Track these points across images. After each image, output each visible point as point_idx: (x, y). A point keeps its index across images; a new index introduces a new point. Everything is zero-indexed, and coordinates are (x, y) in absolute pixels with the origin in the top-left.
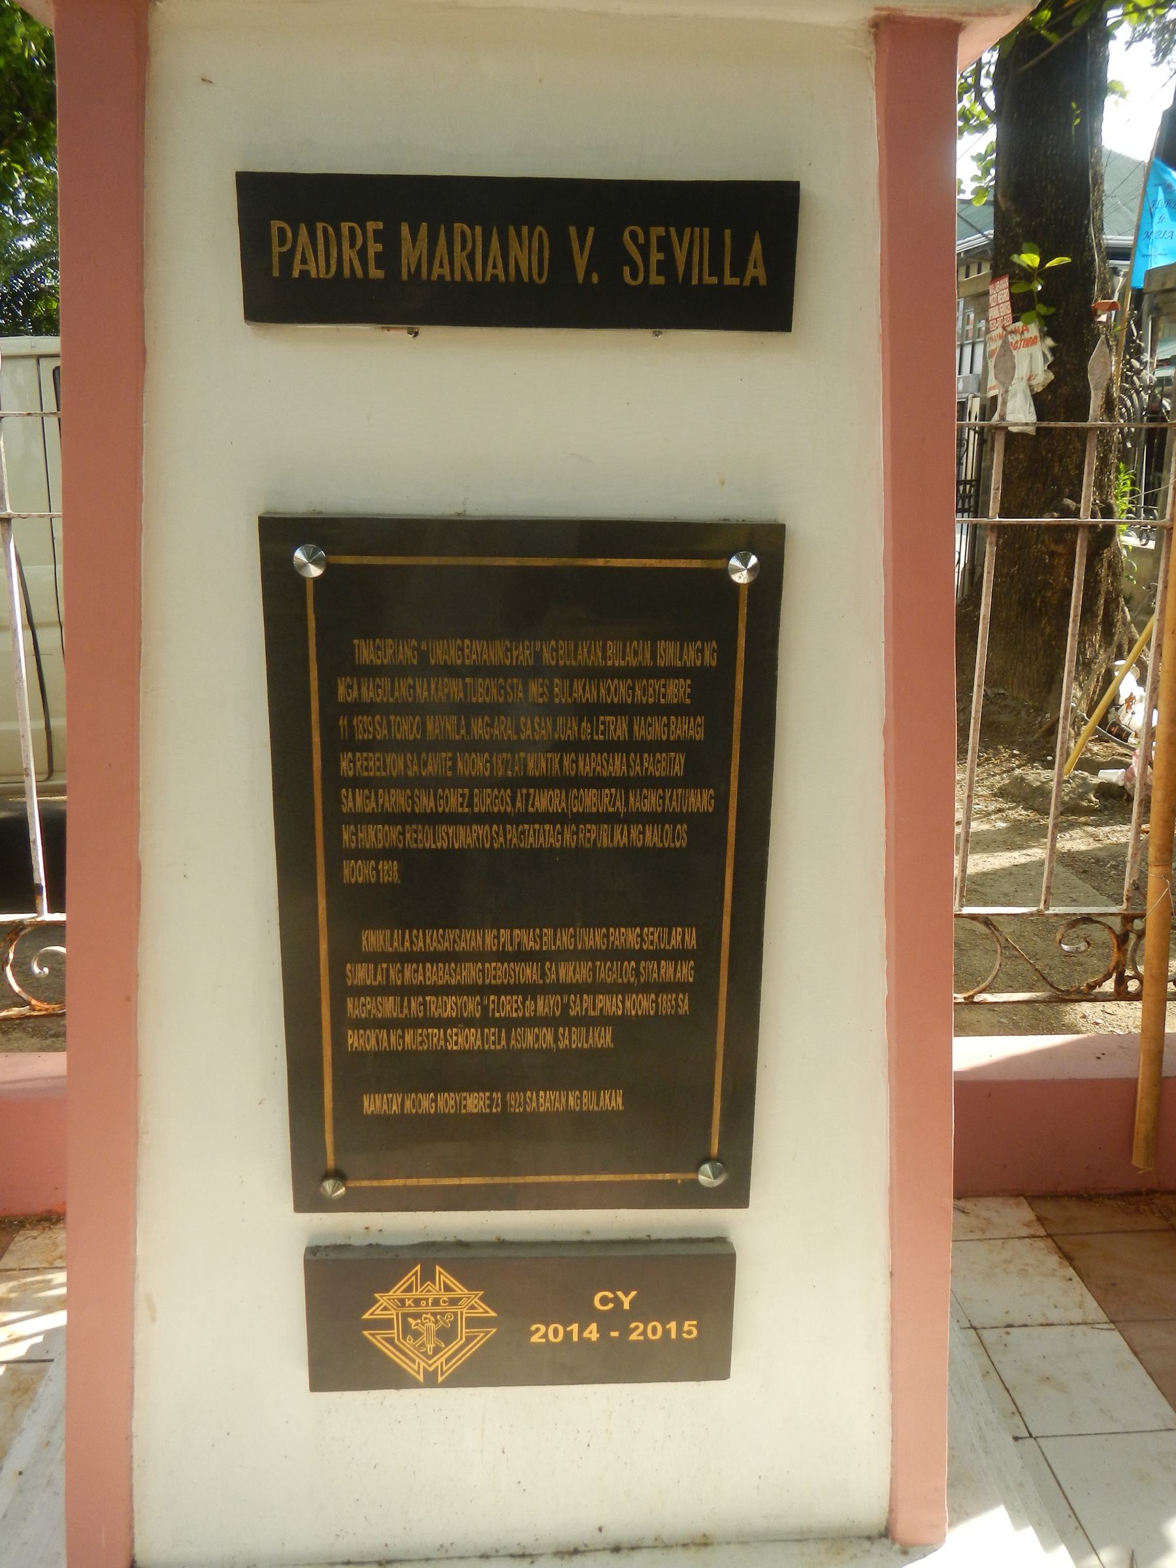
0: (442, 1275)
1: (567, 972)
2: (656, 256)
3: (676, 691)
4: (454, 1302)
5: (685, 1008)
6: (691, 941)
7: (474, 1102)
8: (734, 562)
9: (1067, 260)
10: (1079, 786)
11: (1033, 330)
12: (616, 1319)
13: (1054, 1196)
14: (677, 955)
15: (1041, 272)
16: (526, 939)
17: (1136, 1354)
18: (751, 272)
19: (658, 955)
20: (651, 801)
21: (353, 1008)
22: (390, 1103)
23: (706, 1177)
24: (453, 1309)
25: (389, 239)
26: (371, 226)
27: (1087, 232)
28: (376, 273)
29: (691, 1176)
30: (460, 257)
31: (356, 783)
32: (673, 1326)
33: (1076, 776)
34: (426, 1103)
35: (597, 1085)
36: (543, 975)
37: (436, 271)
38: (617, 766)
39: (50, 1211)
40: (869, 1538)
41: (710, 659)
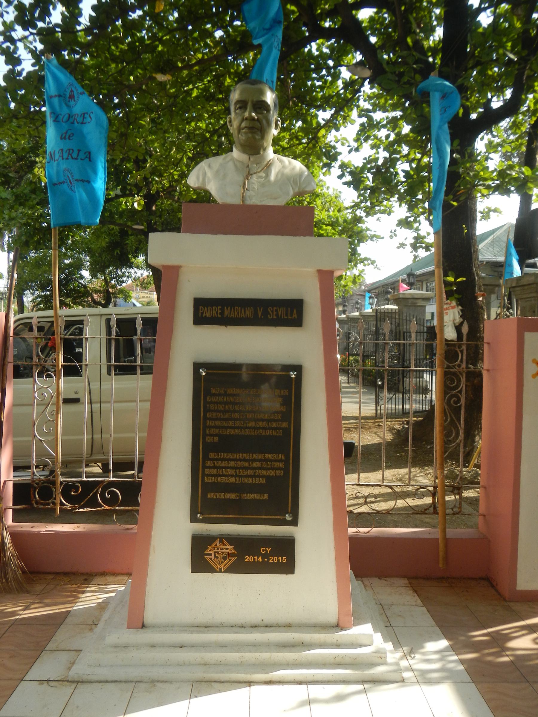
0: (224, 542)
1: (255, 464)
2: (275, 313)
4: (227, 549)
5: (282, 474)
6: (283, 458)
7: (233, 496)
8: (291, 373)
9: (464, 279)
10: (474, 474)
11: (454, 303)
12: (266, 556)
13: (416, 578)
14: (280, 461)
15: (455, 283)
16: (246, 456)
17: (429, 612)
18: (294, 316)
19: (276, 461)
20: (274, 425)
21: (207, 471)
22: (214, 495)
23: (288, 518)
24: (227, 551)
25: (222, 310)
26: (219, 307)
27: (472, 269)
28: (219, 316)
29: (284, 517)
30: (236, 313)
32: (280, 558)
33: (473, 470)
35: (262, 493)
36: (250, 465)
37: (231, 316)
39: (104, 572)
40: (333, 627)
41: (287, 394)
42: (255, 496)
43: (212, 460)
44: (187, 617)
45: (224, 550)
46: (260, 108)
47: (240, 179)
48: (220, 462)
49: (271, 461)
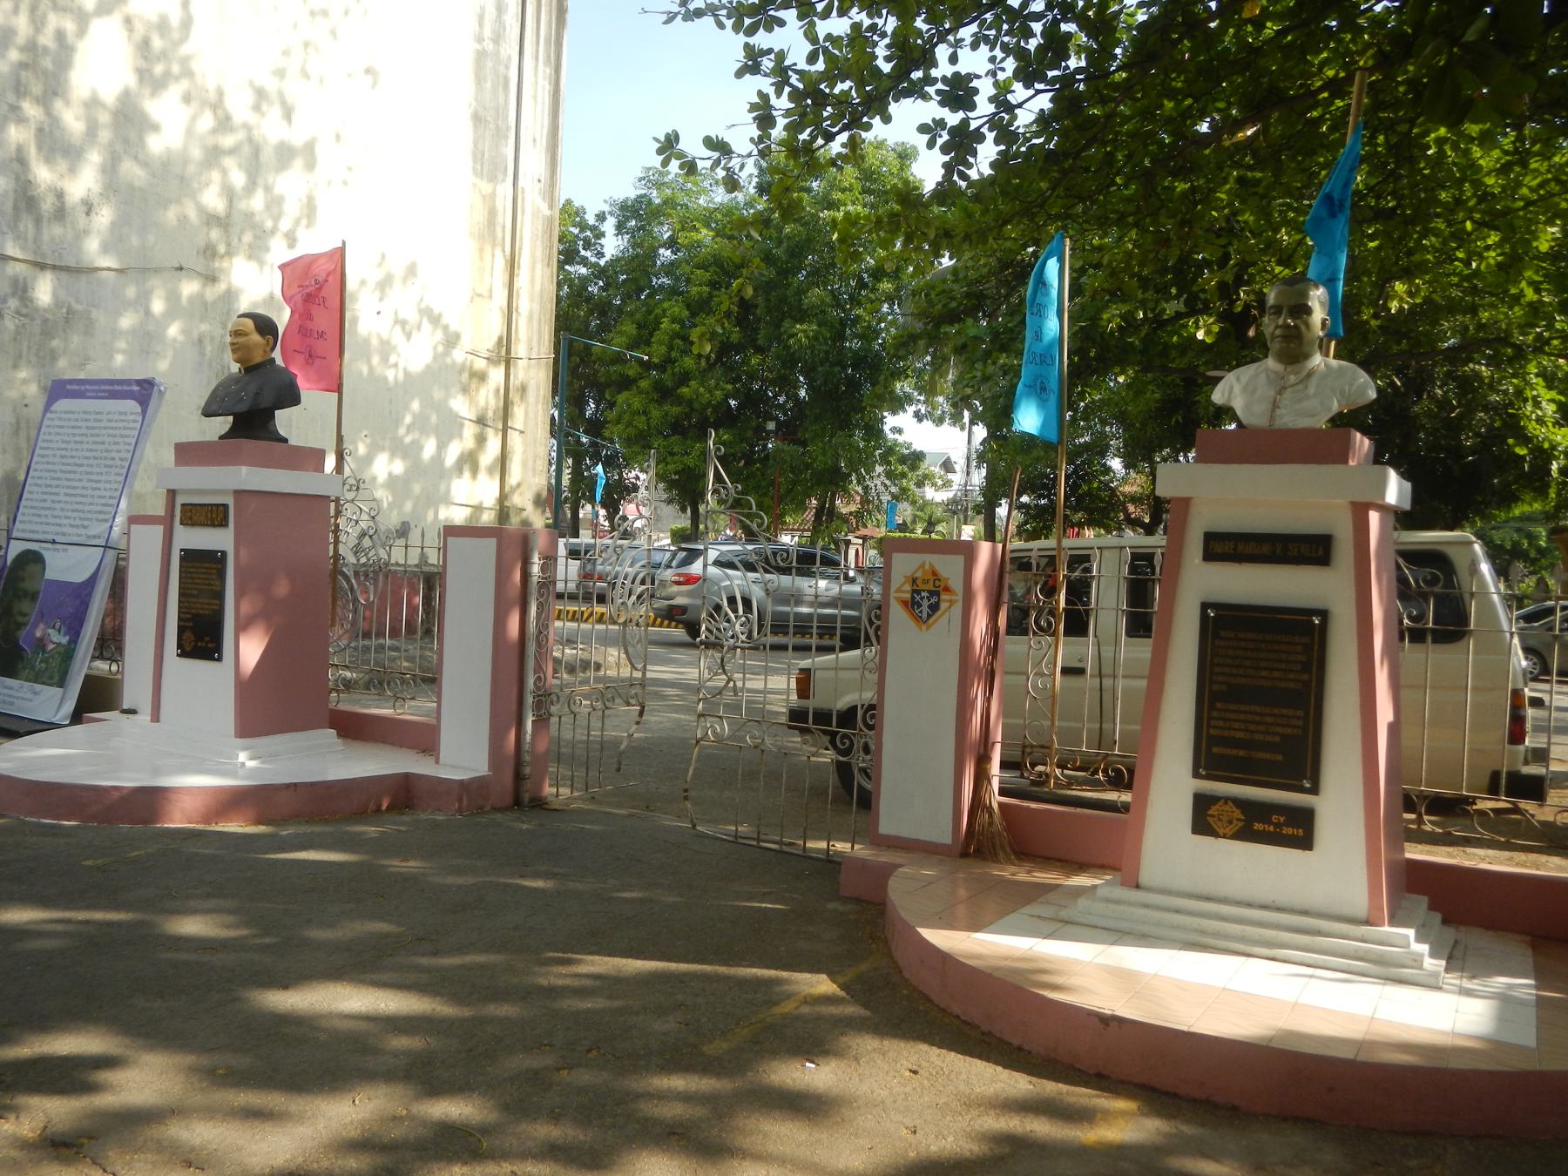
0: (1230, 803)
1: (1269, 719)
3: (1299, 648)
7: (1242, 753)
12: (1278, 825)
14: (1298, 718)
16: (1258, 709)
20: (1292, 676)
21: (1213, 723)
34: (1228, 751)
38: (1283, 666)
42: (1268, 756)
43: (1219, 710)
44: (1184, 884)
47: (1272, 393)
49: (1289, 717)
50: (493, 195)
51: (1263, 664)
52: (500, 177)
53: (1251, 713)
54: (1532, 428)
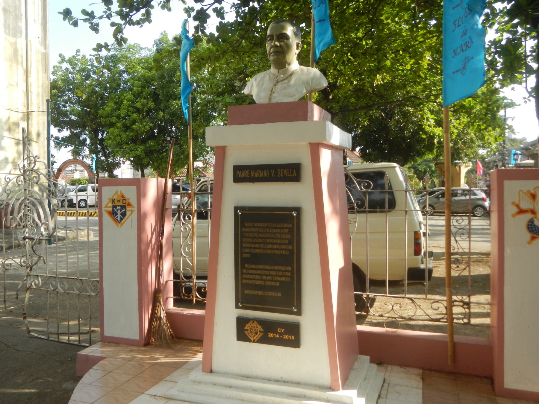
0: (256, 322)
1: (273, 273)
2: (282, 173)
3: (286, 231)
4: (257, 327)
5: (289, 280)
6: (290, 269)
7: (260, 293)
12: (281, 334)
13: (431, 370)
14: (288, 271)
16: (267, 267)
19: (285, 271)
20: (283, 247)
21: (244, 276)
25: (250, 172)
28: (248, 176)
30: (258, 174)
31: (245, 242)
32: (290, 336)
43: (247, 269)
44: (236, 370)
45: (256, 328)
46: (282, 38)
47: (271, 85)
48: (251, 270)
50: (16, 43)
51: (268, 241)
52: (19, 35)
53: (263, 270)
54: (427, 129)
